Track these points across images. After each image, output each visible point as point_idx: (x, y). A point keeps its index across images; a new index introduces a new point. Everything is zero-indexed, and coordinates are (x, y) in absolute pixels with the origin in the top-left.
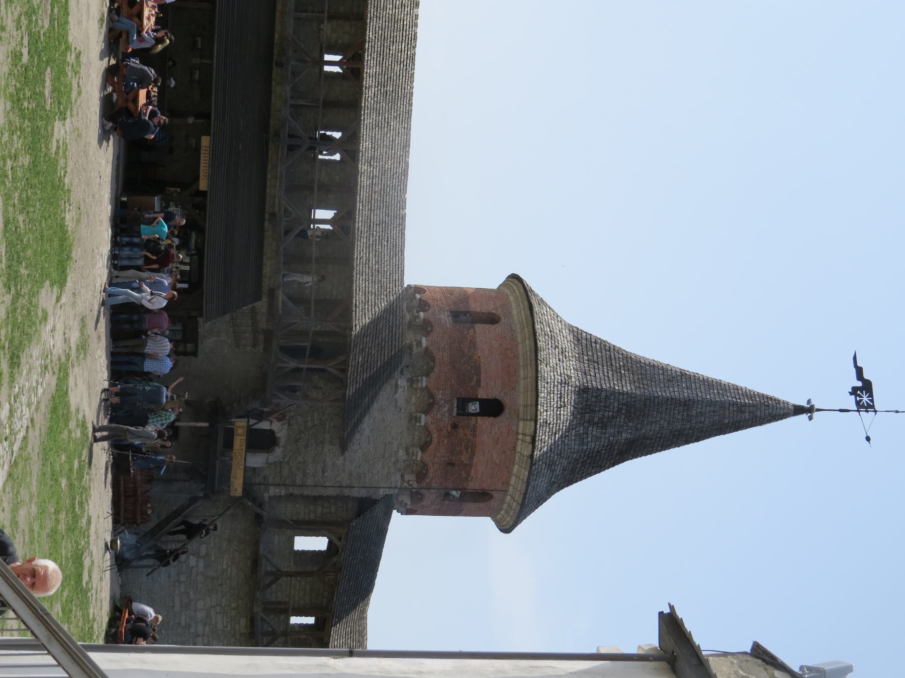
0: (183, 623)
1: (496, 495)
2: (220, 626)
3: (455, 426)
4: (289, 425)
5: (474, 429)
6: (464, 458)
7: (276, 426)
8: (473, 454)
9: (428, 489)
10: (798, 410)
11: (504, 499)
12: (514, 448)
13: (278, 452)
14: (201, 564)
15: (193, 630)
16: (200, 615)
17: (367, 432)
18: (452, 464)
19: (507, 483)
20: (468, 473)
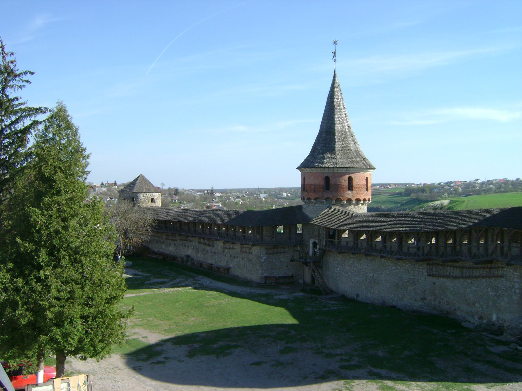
0: (350, 274)
1: (326, 175)
2: (352, 262)
3: (307, 191)
4: (312, 238)
5: (307, 185)
6: (313, 187)
7: (311, 242)
8: (312, 184)
9: (323, 196)
10: (335, 76)
11: (327, 172)
12: (310, 173)
13: (317, 241)
14: (339, 266)
15: (352, 271)
16: (349, 269)
17: (312, 216)
18: (315, 191)
19: (320, 173)
20: (318, 185)
